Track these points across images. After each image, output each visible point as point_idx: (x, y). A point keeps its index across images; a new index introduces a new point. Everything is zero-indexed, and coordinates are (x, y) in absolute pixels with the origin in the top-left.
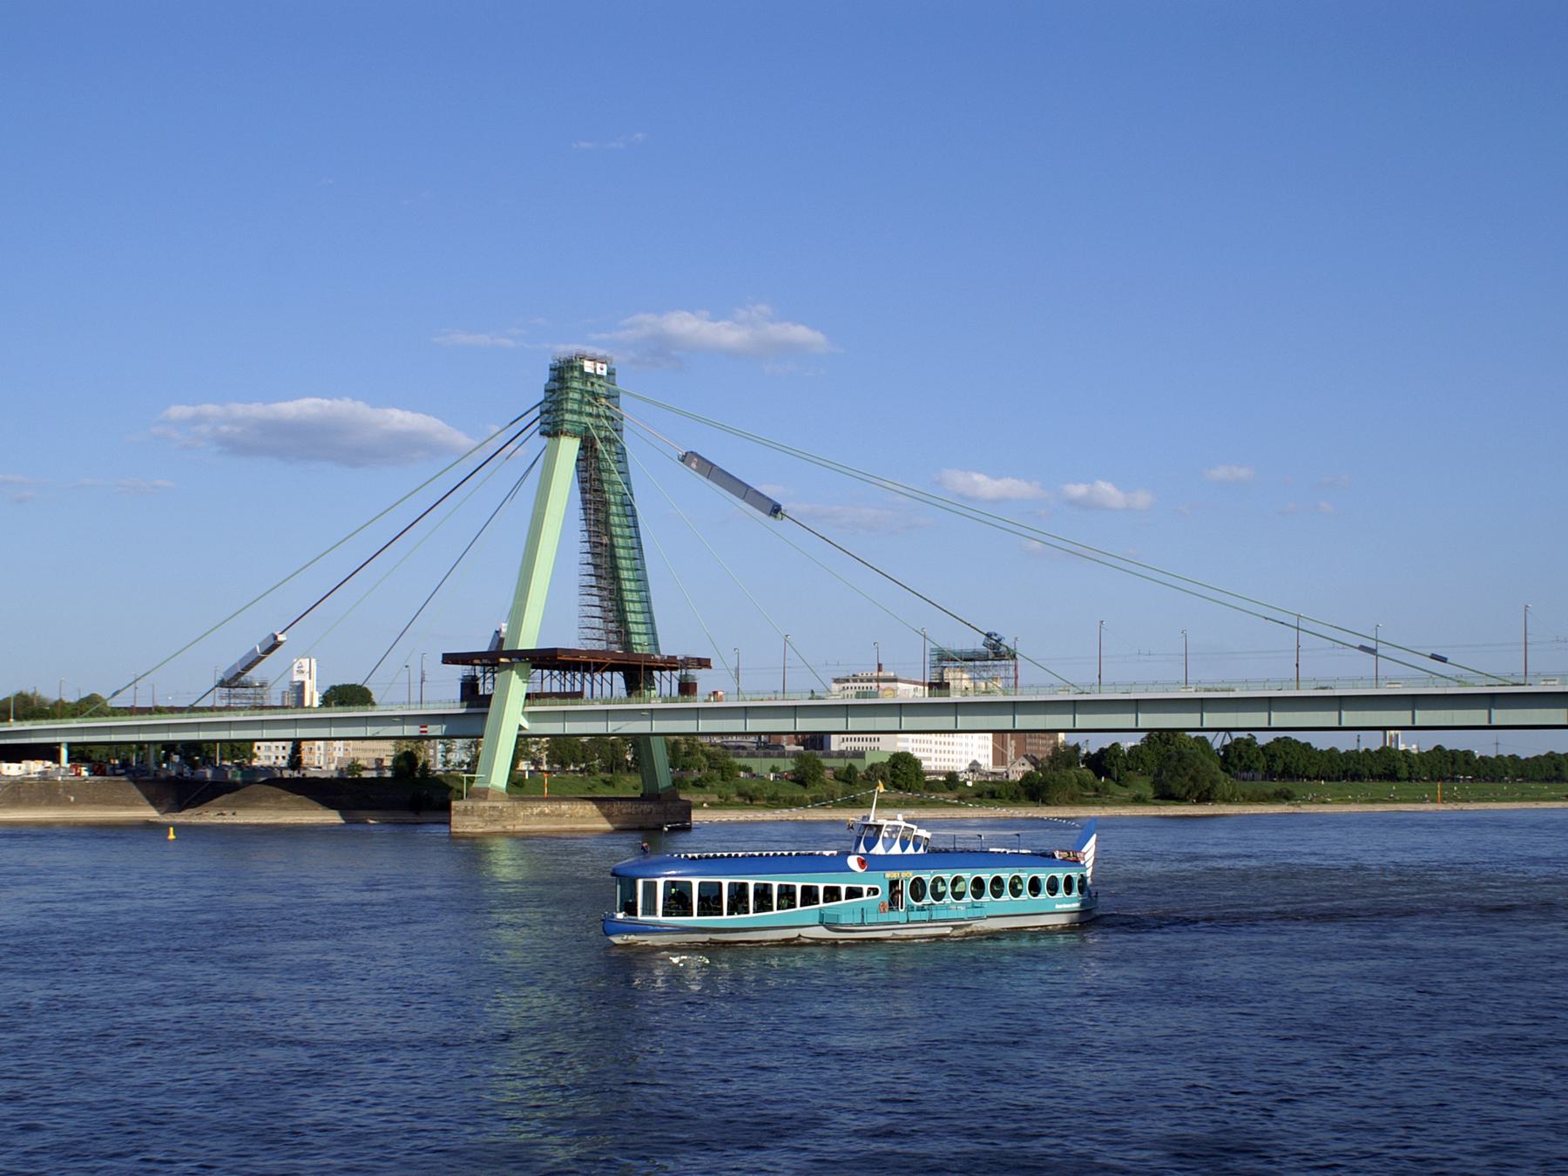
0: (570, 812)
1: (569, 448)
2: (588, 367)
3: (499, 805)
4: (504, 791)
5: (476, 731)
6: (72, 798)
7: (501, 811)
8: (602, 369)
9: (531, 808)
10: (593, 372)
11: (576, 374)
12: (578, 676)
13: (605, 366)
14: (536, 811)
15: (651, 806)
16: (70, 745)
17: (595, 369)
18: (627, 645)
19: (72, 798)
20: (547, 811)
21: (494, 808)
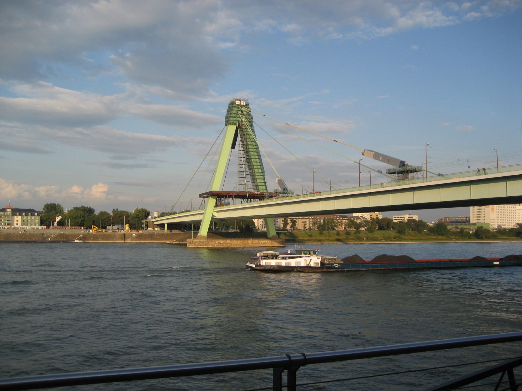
0: (231, 243)
1: (232, 129)
2: (238, 103)
3: (202, 240)
4: (276, 234)
5: (212, 220)
6: (159, 238)
7: (203, 242)
8: (243, 103)
9: (215, 241)
10: (240, 104)
11: (235, 105)
12: (251, 199)
13: (245, 102)
14: (217, 242)
15: (266, 241)
16: (168, 224)
17: (241, 103)
18: (258, 190)
19: (159, 238)
20: (221, 242)
21: (200, 241)
